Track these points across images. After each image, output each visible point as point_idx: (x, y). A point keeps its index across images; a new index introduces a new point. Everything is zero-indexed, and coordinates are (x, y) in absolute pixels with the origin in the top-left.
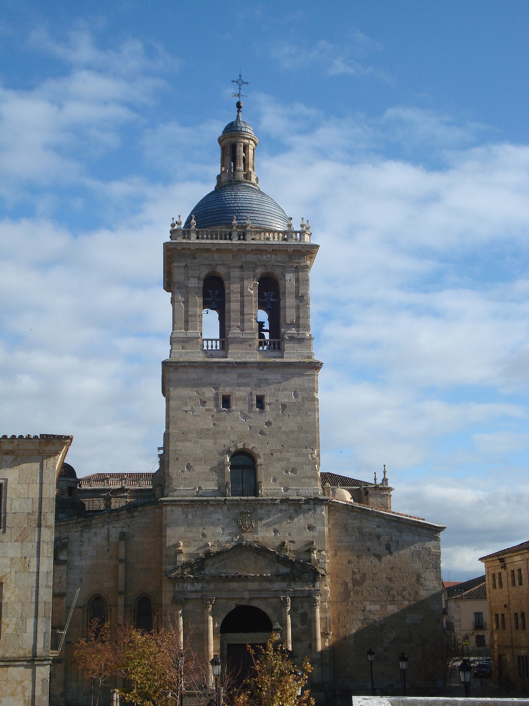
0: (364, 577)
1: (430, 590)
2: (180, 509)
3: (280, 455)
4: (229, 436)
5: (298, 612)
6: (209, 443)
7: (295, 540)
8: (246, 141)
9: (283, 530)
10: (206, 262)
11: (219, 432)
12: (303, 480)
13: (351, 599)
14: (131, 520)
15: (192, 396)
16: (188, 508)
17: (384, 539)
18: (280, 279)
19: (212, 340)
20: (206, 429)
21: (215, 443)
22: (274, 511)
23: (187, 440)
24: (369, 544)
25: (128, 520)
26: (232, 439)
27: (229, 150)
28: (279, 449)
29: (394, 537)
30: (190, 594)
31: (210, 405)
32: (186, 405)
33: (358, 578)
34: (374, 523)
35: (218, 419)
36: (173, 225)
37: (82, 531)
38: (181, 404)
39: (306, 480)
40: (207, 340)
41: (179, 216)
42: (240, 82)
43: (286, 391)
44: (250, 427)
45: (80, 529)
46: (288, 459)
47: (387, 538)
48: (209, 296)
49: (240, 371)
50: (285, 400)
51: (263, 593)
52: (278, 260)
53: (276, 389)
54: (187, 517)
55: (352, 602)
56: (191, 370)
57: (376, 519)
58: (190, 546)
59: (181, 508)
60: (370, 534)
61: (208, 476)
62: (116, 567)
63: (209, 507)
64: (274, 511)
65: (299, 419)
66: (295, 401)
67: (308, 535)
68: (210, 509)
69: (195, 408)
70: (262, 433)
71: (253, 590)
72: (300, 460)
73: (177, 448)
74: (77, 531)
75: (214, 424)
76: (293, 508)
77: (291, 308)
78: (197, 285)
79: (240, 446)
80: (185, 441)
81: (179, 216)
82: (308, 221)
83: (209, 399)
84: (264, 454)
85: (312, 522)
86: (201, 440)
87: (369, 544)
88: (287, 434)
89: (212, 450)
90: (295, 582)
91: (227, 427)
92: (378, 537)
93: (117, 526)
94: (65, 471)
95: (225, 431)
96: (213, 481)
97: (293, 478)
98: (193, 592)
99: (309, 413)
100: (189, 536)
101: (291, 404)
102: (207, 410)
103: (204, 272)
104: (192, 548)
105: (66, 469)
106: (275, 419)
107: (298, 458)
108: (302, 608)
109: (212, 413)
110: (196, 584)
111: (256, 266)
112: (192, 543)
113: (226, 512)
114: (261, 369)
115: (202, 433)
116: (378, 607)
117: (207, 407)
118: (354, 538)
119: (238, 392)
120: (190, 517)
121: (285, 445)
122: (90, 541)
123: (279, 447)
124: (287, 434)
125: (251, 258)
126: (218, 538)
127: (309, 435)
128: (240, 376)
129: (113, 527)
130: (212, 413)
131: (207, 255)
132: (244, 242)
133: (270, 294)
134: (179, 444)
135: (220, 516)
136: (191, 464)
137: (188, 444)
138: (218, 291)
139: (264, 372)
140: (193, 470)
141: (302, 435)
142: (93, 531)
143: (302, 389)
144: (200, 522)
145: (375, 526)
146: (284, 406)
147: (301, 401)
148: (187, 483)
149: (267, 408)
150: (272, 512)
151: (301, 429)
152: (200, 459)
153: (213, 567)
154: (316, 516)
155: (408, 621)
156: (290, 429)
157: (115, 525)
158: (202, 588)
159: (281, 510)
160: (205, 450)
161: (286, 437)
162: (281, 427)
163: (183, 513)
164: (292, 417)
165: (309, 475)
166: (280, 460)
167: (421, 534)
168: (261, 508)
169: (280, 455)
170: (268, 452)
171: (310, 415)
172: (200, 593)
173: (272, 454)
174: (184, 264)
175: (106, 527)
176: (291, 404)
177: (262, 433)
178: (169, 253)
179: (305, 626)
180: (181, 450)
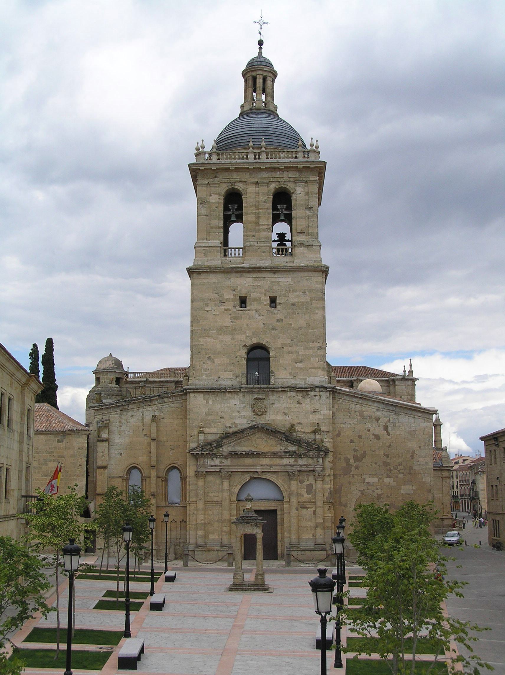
0: (364, 455)
1: (423, 465)
2: (202, 395)
3: (290, 349)
4: (245, 332)
5: (304, 484)
6: (227, 339)
7: (302, 422)
8: (265, 74)
9: (292, 414)
10: (226, 180)
11: (235, 329)
13: (352, 473)
14: (161, 405)
16: (209, 395)
17: (383, 421)
18: (293, 193)
19: (235, 249)
20: (225, 326)
21: (233, 339)
22: (284, 397)
24: (369, 425)
25: (160, 405)
27: (250, 82)
29: (391, 419)
30: (210, 467)
31: (229, 306)
32: (208, 306)
33: (359, 455)
34: (374, 407)
36: (197, 149)
37: (121, 414)
40: (231, 249)
41: (203, 141)
42: (261, 23)
44: (264, 324)
45: (119, 412)
46: (298, 352)
47: (386, 420)
48: (229, 210)
49: (255, 275)
51: (273, 467)
52: (290, 176)
54: (207, 402)
55: (353, 475)
56: (212, 275)
57: (376, 404)
59: (203, 395)
60: (370, 417)
62: (149, 445)
63: (227, 394)
64: (284, 397)
65: (307, 316)
67: (314, 418)
68: (228, 395)
71: (264, 466)
73: (199, 343)
74: (117, 414)
76: (301, 395)
77: (301, 218)
78: (218, 200)
79: (255, 341)
81: (203, 141)
82: (317, 141)
83: (228, 300)
85: (317, 406)
86: (220, 336)
87: (369, 425)
89: (230, 345)
90: (301, 458)
91: (243, 324)
92: (378, 420)
93: (150, 409)
94: (113, 364)
98: (212, 466)
99: (316, 312)
102: (225, 310)
103: (224, 189)
105: (113, 362)
106: (286, 317)
108: (308, 480)
110: (215, 459)
111: (269, 183)
112: (212, 424)
113: (241, 398)
114: (274, 273)
115: (221, 330)
116: (376, 480)
118: (356, 420)
120: (210, 402)
122: (128, 422)
123: (288, 341)
125: (265, 175)
126: (234, 420)
127: (315, 330)
128: (255, 279)
129: (147, 411)
130: (230, 312)
131: (227, 174)
132: (259, 161)
133: (283, 206)
134: (201, 340)
135: (237, 402)
137: (209, 340)
138: (237, 205)
139: (276, 276)
140: (214, 362)
141: (310, 331)
142: (130, 413)
143: (310, 290)
144: (219, 406)
145: (375, 410)
147: (309, 300)
149: (278, 307)
150: (282, 398)
151: (308, 325)
153: (230, 444)
154: (321, 402)
155: (402, 492)
157: (148, 409)
158: (220, 463)
160: (224, 345)
161: (295, 333)
162: (291, 324)
163: (204, 400)
165: (316, 366)
166: (290, 353)
167: (415, 417)
168: (273, 395)
169: (290, 349)
170: (279, 346)
171: (317, 313)
172: (218, 467)
173: (283, 347)
174: (207, 182)
175: (141, 410)
178: (194, 173)
179: (310, 496)
180: (203, 345)
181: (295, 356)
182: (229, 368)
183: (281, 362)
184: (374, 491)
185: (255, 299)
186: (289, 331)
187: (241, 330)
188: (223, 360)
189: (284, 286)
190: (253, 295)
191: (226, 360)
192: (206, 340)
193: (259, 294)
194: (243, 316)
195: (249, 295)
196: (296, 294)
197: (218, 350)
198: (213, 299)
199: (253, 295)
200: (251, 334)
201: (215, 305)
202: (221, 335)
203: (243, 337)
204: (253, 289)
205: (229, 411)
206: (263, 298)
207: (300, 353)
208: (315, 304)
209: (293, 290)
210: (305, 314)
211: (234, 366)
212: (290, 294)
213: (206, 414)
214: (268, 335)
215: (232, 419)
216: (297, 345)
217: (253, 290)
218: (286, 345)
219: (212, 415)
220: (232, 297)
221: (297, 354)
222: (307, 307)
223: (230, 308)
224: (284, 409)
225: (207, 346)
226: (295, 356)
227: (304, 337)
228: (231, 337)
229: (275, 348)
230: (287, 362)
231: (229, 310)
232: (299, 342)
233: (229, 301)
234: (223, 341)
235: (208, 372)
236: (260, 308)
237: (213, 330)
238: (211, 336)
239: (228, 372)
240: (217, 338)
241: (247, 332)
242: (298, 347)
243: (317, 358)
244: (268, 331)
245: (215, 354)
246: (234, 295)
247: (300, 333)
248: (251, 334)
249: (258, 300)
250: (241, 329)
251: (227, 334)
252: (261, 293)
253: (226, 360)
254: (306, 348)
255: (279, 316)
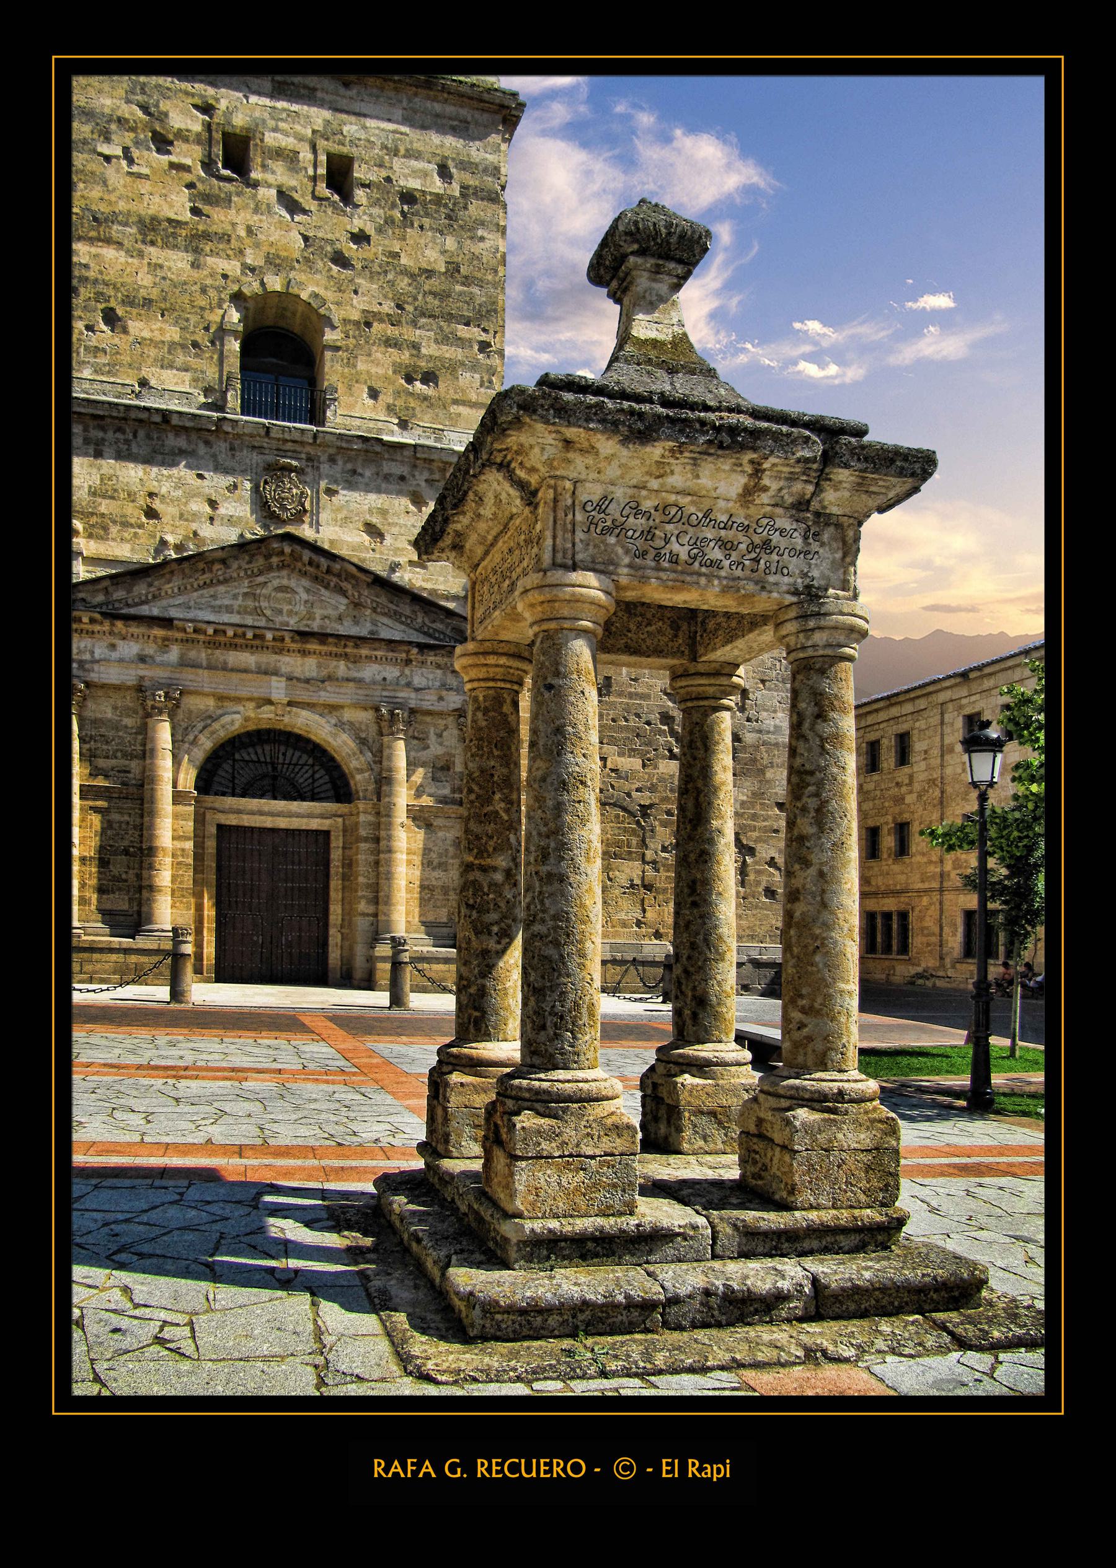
3: (391, 331)
4: (241, 252)
6: (178, 262)
9: (395, 530)
11: (206, 236)
12: (454, 409)
15: (127, 116)
20: (170, 221)
21: (195, 265)
23: (108, 241)
26: (249, 261)
28: (388, 315)
31: (189, 155)
35: (209, 199)
38: (92, 132)
39: (461, 409)
43: (417, 159)
44: (306, 239)
46: (416, 346)
50: (414, 184)
53: (386, 148)
58: (107, 539)
61: (169, 352)
66: (442, 192)
69: (135, 153)
70: (340, 260)
72: (450, 352)
75: (195, 211)
80: (100, 244)
83: (182, 135)
84: (344, 320)
86: (152, 249)
88: (412, 276)
89: (185, 283)
91: (234, 225)
95: (229, 236)
96: (186, 370)
97: (426, 398)
100: (103, 509)
101: (428, 198)
102: (172, 165)
104: (112, 544)
106: (380, 230)
107: (445, 348)
109: (188, 177)
117: (173, 158)
119: (272, 134)
121: (406, 306)
123: (388, 307)
124: (412, 276)
126: (194, 526)
136: (120, 312)
137: (109, 253)
140: (125, 331)
146: (408, 197)
148: (104, 365)
150: (361, 475)
152: (148, 302)
156: (425, 266)
159: (390, 475)
160: (164, 278)
161: (410, 285)
162: (397, 256)
164: (430, 233)
166: (389, 343)
169: (391, 331)
173: (368, 325)
176: (428, 198)
177: (340, 260)
180: (86, 266)
181: (405, 356)
182: (181, 358)
183: (361, 366)
184: (629, 795)
185: (279, 153)
186: (390, 276)
187: (229, 241)
188: (161, 329)
189: (377, 132)
190: (271, 139)
191: (173, 333)
192: (99, 250)
193: (291, 140)
194: (235, 199)
195: (258, 135)
196: (413, 163)
197: (143, 293)
198: (127, 121)
199: (271, 139)
200: (260, 262)
201: (137, 143)
202: (153, 243)
203: (233, 267)
204: (273, 118)
205: (179, 493)
206: (306, 155)
207: (424, 351)
208: (476, 209)
209: (407, 150)
210: (441, 233)
211: (197, 356)
212: (397, 163)
213: (93, 493)
214: (318, 276)
215: (187, 520)
216: (414, 324)
217: (271, 123)
218: (379, 317)
219: (112, 498)
220: (197, 128)
221: (414, 352)
222: (451, 214)
223: (188, 161)
224: (370, 510)
225: (101, 273)
226: (405, 356)
227: (437, 302)
228: (190, 257)
229: (345, 321)
230: (381, 371)
231: (186, 168)
232: (423, 315)
233: (186, 140)
234: (161, 267)
235: (103, 360)
236: (293, 183)
237: (126, 224)
238: (120, 244)
239: (175, 371)
240: (141, 254)
241: (248, 251)
242: (418, 332)
243: (477, 376)
244: (320, 265)
245: (132, 304)
246: (208, 127)
247: (427, 288)
248: (260, 262)
249: (290, 158)
250: (225, 238)
251: (175, 247)
252: (300, 138)
253: (173, 333)
254: (445, 339)
255: (358, 223)
